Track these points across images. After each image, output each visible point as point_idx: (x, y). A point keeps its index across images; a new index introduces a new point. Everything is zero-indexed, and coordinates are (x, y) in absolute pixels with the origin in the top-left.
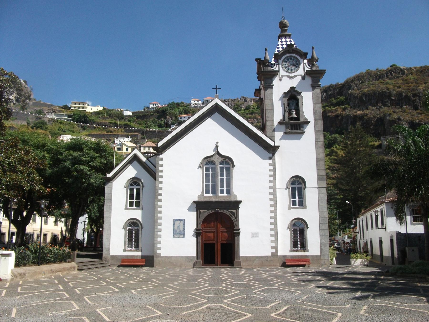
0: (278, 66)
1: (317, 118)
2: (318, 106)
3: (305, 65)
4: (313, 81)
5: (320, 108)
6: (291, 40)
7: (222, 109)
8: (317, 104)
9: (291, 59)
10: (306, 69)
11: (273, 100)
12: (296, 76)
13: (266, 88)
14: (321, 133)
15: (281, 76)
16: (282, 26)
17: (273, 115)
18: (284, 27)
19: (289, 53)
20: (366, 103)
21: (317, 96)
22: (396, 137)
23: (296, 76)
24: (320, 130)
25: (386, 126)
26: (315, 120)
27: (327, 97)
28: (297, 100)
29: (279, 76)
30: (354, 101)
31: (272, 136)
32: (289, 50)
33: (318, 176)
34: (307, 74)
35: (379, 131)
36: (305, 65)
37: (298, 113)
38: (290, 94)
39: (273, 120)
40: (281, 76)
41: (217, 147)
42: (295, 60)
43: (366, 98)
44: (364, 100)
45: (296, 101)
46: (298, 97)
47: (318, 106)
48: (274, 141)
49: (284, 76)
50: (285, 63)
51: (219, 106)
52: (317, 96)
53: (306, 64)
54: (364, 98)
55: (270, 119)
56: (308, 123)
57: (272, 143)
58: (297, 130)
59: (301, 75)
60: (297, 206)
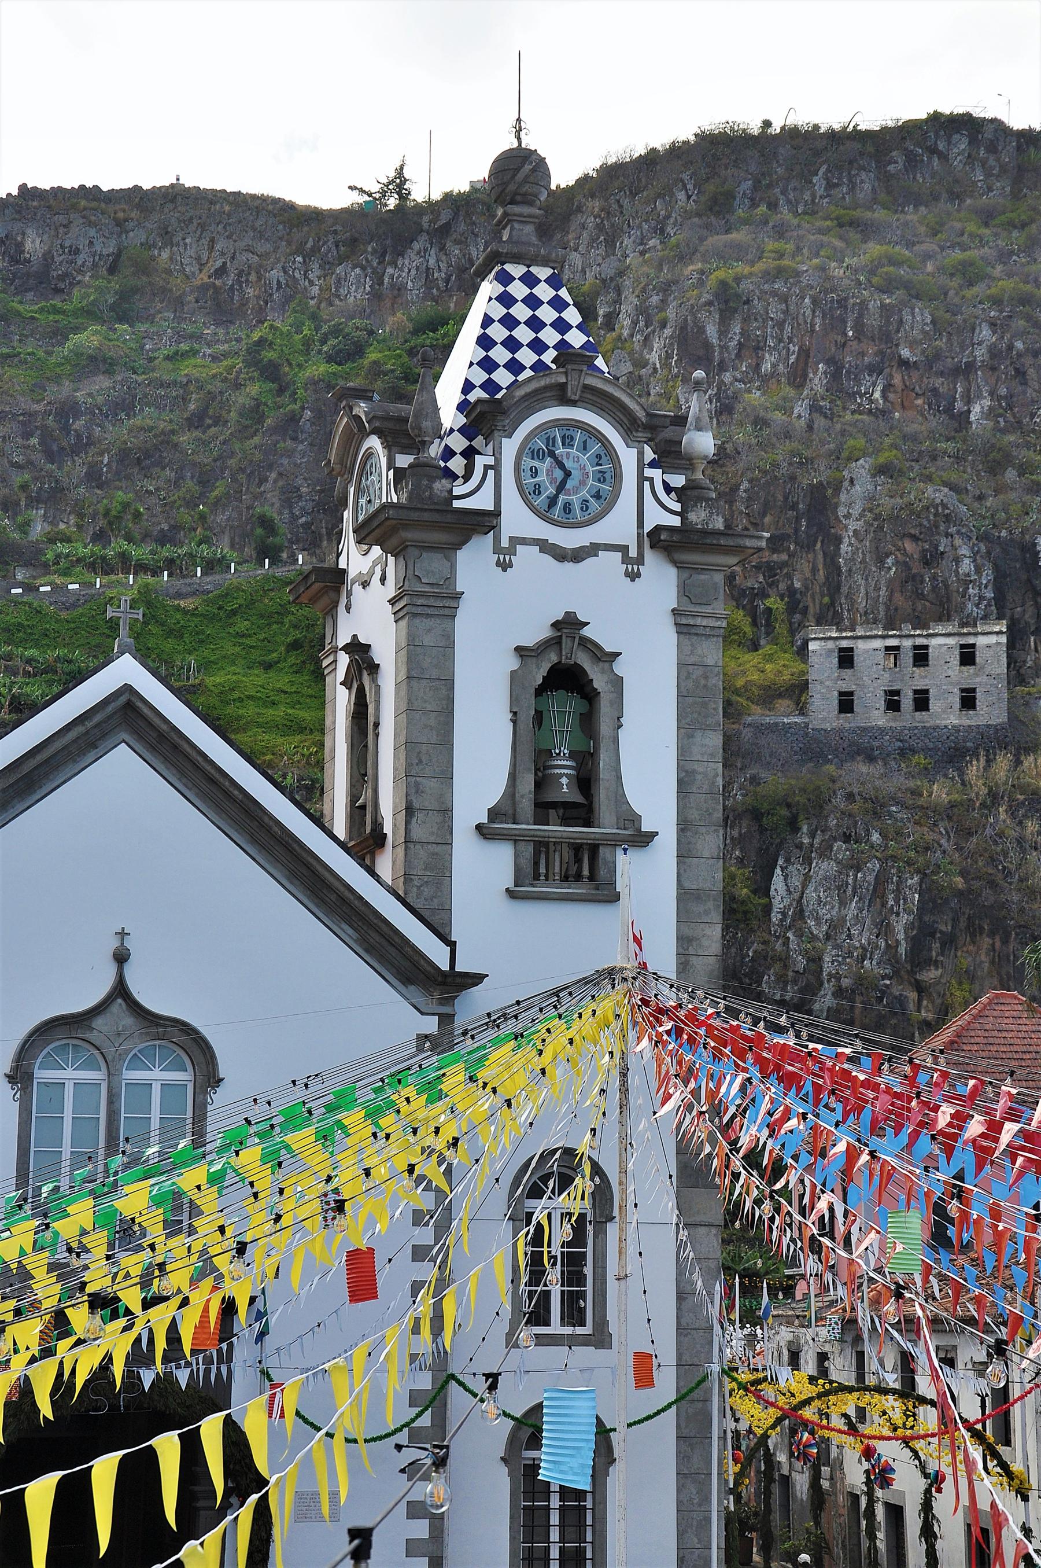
0: (491, 473)
1: (694, 815)
2: (707, 741)
3: (647, 484)
4: (684, 591)
5: (712, 755)
6: (564, 293)
7: (164, 727)
8: (698, 734)
9: (572, 439)
10: (656, 517)
11: (450, 684)
12: (594, 550)
13: (419, 610)
14: (710, 905)
15: (505, 543)
16: (512, 187)
17: (447, 777)
18: (525, 195)
19: (565, 400)
20: (722, 367)
21: (703, 682)
22: (908, 643)
23: (594, 550)
24: (708, 885)
25: (844, 547)
26: (684, 826)
27: (447, 280)
28: (588, 695)
29: (497, 540)
30: (638, 337)
31: (435, 904)
32: (563, 387)
33: (681, 1157)
34: (652, 547)
35: (797, 585)
36: (647, 484)
37: (586, 782)
38: (554, 658)
39: (446, 812)
40: (505, 543)
41: (121, 958)
42: (595, 448)
43: (723, 333)
44: (707, 345)
45: (583, 706)
46: (599, 682)
47: (707, 741)
48: (452, 945)
49: (523, 541)
50: (536, 463)
51: (146, 710)
52: (703, 682)
53: (651, 480)
54: (712, 331)
55: (427, 804)
56: (643, 839)
57: (437, 954)
58: (578, 877)
59: (624, 549)
60: (556, 1328)
